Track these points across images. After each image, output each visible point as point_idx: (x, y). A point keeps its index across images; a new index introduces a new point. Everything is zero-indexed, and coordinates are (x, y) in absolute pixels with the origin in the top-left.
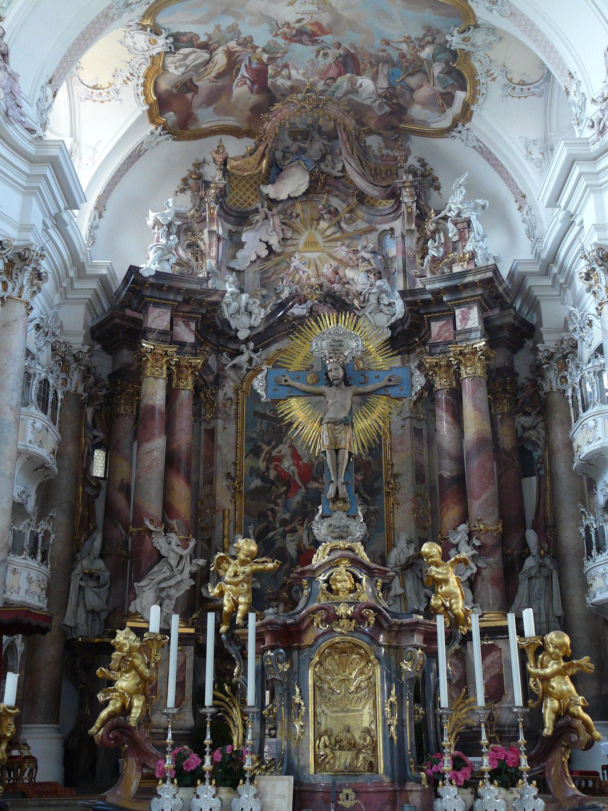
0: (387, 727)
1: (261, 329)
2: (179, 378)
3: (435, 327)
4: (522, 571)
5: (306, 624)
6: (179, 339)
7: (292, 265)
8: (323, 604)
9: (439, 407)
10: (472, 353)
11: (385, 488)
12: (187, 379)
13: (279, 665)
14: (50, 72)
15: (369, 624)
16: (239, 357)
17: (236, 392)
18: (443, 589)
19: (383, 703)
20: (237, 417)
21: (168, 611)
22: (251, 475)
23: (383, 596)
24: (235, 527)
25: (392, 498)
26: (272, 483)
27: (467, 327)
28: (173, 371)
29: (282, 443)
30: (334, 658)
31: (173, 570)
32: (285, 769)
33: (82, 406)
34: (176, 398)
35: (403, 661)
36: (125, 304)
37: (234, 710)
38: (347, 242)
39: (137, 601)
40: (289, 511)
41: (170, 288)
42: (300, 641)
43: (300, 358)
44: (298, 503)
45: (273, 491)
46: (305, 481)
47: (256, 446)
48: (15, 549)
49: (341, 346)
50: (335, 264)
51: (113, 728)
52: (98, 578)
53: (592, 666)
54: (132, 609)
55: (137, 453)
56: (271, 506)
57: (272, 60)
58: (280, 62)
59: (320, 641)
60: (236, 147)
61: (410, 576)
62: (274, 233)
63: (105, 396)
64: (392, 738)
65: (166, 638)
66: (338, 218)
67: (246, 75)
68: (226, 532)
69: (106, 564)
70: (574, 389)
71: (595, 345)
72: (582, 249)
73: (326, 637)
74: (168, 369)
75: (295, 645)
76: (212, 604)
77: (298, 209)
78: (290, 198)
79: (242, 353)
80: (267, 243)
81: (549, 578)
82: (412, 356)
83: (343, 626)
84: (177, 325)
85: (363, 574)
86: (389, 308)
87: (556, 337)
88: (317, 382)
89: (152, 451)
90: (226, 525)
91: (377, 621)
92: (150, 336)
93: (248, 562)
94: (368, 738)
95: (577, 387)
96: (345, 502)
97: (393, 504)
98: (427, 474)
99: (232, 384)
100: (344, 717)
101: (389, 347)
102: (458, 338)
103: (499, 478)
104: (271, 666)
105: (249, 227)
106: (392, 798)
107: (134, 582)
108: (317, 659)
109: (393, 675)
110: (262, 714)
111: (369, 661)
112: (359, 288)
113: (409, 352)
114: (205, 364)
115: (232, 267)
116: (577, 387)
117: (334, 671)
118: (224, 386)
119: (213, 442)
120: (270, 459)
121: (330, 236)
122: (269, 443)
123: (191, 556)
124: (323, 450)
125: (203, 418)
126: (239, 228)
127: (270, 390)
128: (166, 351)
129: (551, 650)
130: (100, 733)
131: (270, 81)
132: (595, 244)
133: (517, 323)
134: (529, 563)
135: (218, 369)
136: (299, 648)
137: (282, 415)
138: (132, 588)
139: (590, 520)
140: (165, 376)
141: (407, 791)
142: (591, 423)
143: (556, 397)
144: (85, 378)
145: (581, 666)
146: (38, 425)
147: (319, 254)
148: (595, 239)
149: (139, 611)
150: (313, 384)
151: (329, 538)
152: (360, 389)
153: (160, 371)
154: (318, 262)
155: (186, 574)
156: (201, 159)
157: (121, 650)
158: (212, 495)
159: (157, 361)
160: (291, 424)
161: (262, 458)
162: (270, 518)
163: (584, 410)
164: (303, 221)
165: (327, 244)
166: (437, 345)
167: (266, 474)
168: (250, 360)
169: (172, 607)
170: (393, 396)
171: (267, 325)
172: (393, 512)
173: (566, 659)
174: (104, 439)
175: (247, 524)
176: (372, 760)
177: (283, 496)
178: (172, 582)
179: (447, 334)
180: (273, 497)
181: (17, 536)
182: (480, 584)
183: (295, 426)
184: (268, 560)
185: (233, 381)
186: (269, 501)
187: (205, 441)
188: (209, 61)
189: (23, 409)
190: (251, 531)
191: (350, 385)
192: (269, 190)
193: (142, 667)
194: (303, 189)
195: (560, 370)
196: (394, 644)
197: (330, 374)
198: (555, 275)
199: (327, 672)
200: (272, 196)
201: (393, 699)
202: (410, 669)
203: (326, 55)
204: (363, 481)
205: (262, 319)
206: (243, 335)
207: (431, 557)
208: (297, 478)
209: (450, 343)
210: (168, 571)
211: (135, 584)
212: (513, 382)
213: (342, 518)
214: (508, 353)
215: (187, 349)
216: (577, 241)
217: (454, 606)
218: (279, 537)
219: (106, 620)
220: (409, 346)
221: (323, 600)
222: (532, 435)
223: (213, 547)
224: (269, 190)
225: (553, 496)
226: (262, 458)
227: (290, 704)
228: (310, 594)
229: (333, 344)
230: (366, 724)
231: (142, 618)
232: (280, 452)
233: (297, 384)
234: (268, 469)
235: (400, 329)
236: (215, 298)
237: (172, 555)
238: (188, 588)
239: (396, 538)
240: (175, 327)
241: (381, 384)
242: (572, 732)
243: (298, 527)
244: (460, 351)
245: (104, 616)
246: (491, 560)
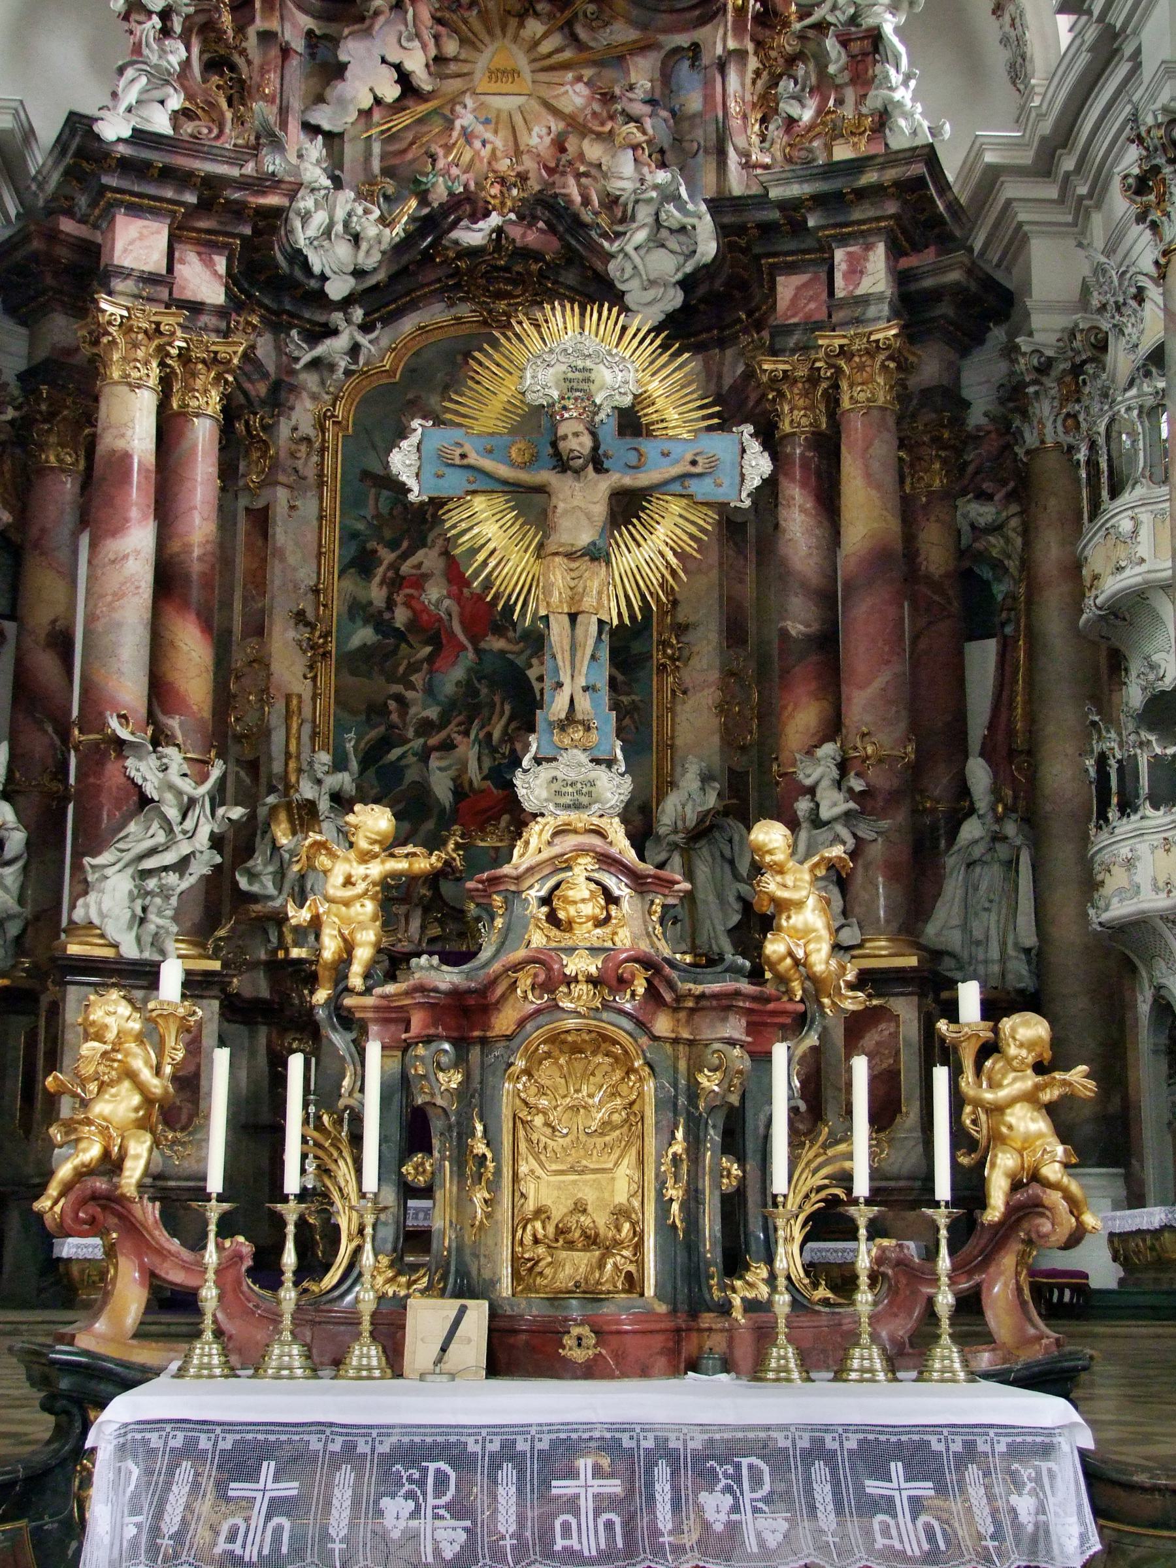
0: (663, 1206)
1: (381, 276)
2: (189, 389)
3: (787, 288)
4: (955, 848)
5: (499, 991)
6: (189, 295)
7: (458, 124)
8: (538, 950)
9: (786, 475)
10: (868, 352)
11: (657, 656)
12: (206, 391)
13: (441, 1075)
15: (633, 994)
16: (328, 342)
18: (792, 921)
19: (659, 1156)
20: (321, 484)
21: (160, 921)
22: (352, 618)
23: (664, 934)
24: (314, 735)
25: (670, 679)
26: (400, 636)
27: (859, 292)
28: (173, 372)
29: (424, 545)
30: (556, 1063)
31: (171, 830)
32: (450, 1287)
34: (181, 435)
35: (701, 1071)
36: (61, 205)
37: (341, 1163)
38: (588, 73)
39: (92, 898)
40: (438, 704)
41: (168, 174)
42: (487, 1026)
43: (497, 404)
44: (458, 684)
45: (401, 653)
46: (475, 640)
47: (364, 548)
49: (587, 380)
50: (557, 126)
51: (82, 1203)
53: (1091, 1084)
54: (79, 915)
55: (89, 562)
56: (397, 688)
59: (529, 1027)
61: (705, 852)
62: (417, 44)
63: (12, 422)
64: (674, 1226)
65: (195, 1013)
66: (568, 14)
68: (293, 748)
69: (17, 813)
70: (1093, 446)
71: (1146, 346)
72: (1134, 118)
73: (541, 1019)
74: (162, 364)
75: (476, 1033)
76: (258, 907)
79: (335, 332)
80: (398, 67)
81: (1011, 865)
82: (729, 352)
83: (579, 997)
84: (182, 262)
85: (623, 886)
86: (682, 238)
87: (1062, 321)
88: (530, 463)
89: (126, 557)
90: (294, 730)
91: (651, 990)
92: (118, 285)
93: (375, 856)
94: (627, 1226)
95: (1101, 441)
96: (588, 729)
97: (673, 691)
98: (752, 626)
99: (309, 404)
100: (575, 1182)
101: (694, 387)
102: (838, 316)
103: (915, 639)
104: (424, 1077)
105: (356, 27)
106: (671, 1344)
107: (85, 855)
108: (521, 1064)
109: (682, 1101)
110: (400, 1174)
111: (630, 1070)
113: (722, 343)
114: (248, 357)
115: (313, 122)
116: (1101, 441)
117: (556, 1089)
118: (292, 408)
119: (265, 536)
120: (395, 582)
121: (549, 55)
122: (393, 545)
123: (212, 800)
124: (542, 612)
125: (241, 483)
126: (331, 29)
127: (427, 474)
128: (158, 324)
129: (1013, 1051)
130: (57, 1209)
132: (1165, 109)
133: (973, 287)
134: (971, 830)
135: (278, 367)
136: (484, 1042)
137: (453, 532)
138: (77, 867)
139: (1110, 743)
140: (153, 381)
141: (700, 1330)
142: (1126, 525)
143: (1051, 463)
145: (1070, 1084)
147: (521, 100)
148: (1164, 98)
149: (96, 921)
150: (523, 466)
151: (551, 807)
152: (628, 481)
153: (144, 371)
154: (518, 119)
155: (203, 838)
157: (99, 1038)
158: (261, 662)
159: (135, 345)
160: (474, 551)
161: (377, 579)
162: (394, 717)
163: (1114, 493)
164: (484, 16)
165: (543, 77)
166: (788, 330)
167: (387, 616)
169: (170, 913)
170: (699, 498)
171: (395, 268)
172: (672, 710)
173: (1040, 1068)
174: (9, 525)
175: (341, 728)
176: (632, 1268)
177: (425, 665)
178: (169, 858)
179: (812, 306)
180: (401, 670)
183: (481, 557)
184: (418, 850)
185: (315, 397)
186: (392, 679)
187: (248, 534)
190: (349, 746)
191: (607, 471)
193: (146, 1075)
195: (1064, 400)
196: (686, 1035)
197: (562, 445)
198: (1067, 175)
199: (542, 1091)
201: (678, 1148)
202: (716, 1089)
205: (383, 253)
206: (337, 289)
207: (770, 852)
208: (457, 628)
209: (818, 326)
210: (161, 832)
211: (87, 860)
212: (958, 421)
213: (580, 765)
216: (1124, 97)
217: (814, 958)
218: (412, 759)
219: (18, 939)
220: (722, 329)
221: (538, 939)
222: (995, 544)
223: (263, 780)
225: (1030, 683)
226: (377, 579)
227: (462, 1156)
228: (507, 929)
229: (570, 375)
230: (621, 1198)
231: (102, 936)
232: (421, 564)
233: (488, 464)
234: (390, 604)
235: (702, 290)
236: (273, 200)
238: (206, 871)
239: (679, 769)
240: (178, 267)
241: (675, 471)
242: (1042, 1215)
243: (458, 738)
244: (841, 347)
245: (13, 929)
246: (885, 824)
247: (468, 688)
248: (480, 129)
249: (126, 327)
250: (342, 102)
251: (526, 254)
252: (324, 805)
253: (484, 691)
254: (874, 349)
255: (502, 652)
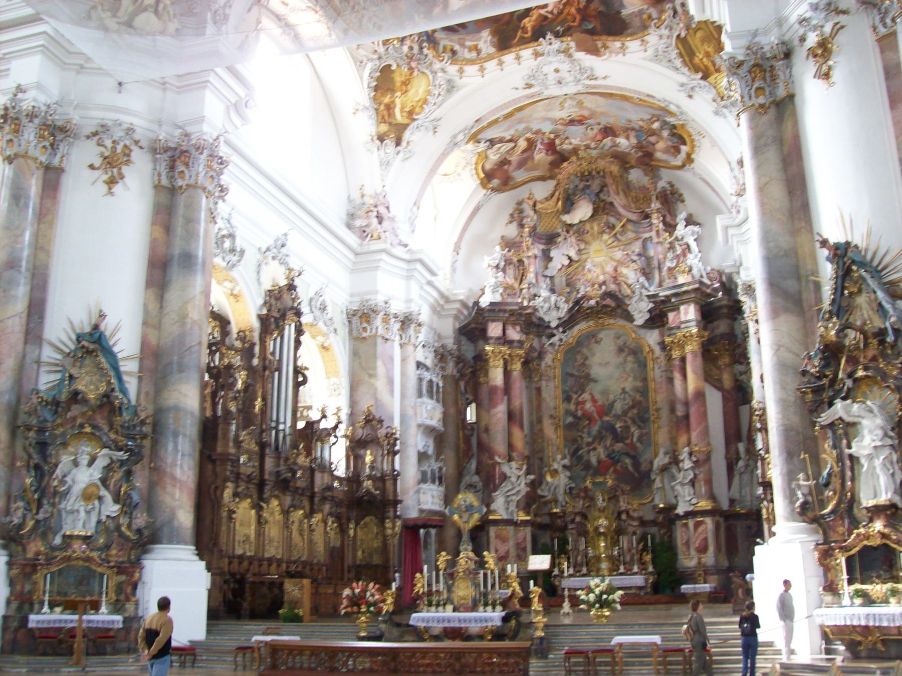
2: (512, 364)
11: (652, 418)
14: (414, 200)
17: (553, 360)
26: (579, 419)
33: (456, 382)
38: (622, 247)
41: (500, 310)
46: (601, 418)
48: (423, 480)
50: (615, 264)
52: (475, 487)
56: (579, 434)
57: (557, 136)
58: (563, 137)
60: (541, 190)
66: (614, 232)
67: (542, 147)
77: (588, 227)
78: (581, 222)
79: (553, 335)
99: (550, 356)
112: (630, 282)
120: (578, 404)
122: (576, 393)
131: (558, 148)
144: (457, 363)
146: (429, 407)
156: (520, 199)
158: (541, 430)
168: (561, 340)
178: (514, 492)
181: (424, 474)
182: (697, 485)
186: (578, 431)
188: (515, 147)
189: (419, 400)
192: (567, 219)
194: (589, 214)
200: (569, 222)
203: (592, 129)
204: (638, 414)
206: (554, 324)
208: (595, 415)
211: (494, 494)
214: (729, 321)
215: (515, 344)
224: (567, 219)
234: (577, 410)
237: (513, 475)
247: (599, 432)
248: (593, 268)
249: (493, 352)
250: (553, 268)
251: (606, 306)
252: (560, 469)
253: (604, 432)
254: (691, 336)
255: (608, 421)
